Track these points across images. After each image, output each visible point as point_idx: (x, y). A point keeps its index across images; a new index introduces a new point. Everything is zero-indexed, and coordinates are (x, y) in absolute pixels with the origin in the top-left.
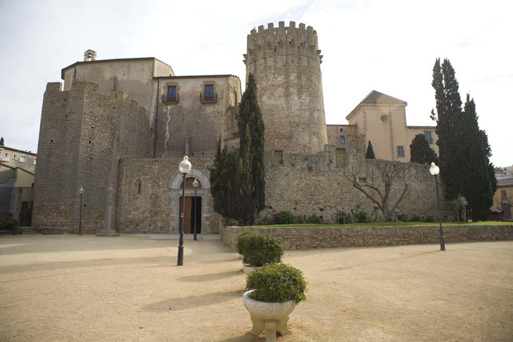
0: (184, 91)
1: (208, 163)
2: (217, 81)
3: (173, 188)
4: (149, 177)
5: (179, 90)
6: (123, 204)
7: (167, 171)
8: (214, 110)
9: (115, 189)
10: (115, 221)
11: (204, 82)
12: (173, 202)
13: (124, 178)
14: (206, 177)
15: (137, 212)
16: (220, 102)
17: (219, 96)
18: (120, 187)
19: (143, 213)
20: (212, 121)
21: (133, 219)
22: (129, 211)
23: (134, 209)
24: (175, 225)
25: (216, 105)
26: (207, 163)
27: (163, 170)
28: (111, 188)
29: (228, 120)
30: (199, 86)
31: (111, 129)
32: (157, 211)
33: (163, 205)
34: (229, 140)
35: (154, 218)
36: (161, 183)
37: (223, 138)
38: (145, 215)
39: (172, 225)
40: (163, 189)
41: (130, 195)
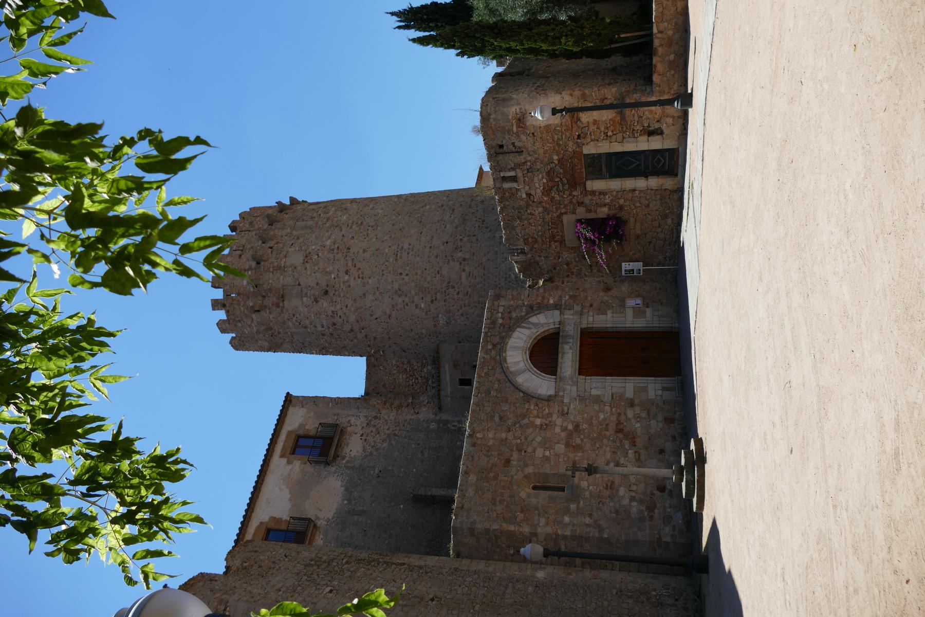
0: (288, 506)
1: (500, 315)
2: (292, 424)
3: (552, 392)
4: (515, 455)
5: (279, 521)
6: (594, 533)
7: (505, 407)
8: (359, 435)
11: (282, 456)
12: (594, 392)
13: (512, 528)
14: (533, 320)
15: (622, 491)
16: (343, 421)
17: (330, 421)
20: (384, 441)
21: (641, 502)
22: (617, 512)
23: (611, 497)
24: (659, 386)
25: (349, 429)
26: (496, 319)
27: (501, 418)
29: (392, 404)
30: (290, 467)
31: (347, 563)
32: (619, 431)
33: (602, 416)
34: (442, 393)
35: (639, 441)
36: (538, 421)
37: (433, 417)
39: (660, 393)
40: (555, 416)
41: (567, 511)
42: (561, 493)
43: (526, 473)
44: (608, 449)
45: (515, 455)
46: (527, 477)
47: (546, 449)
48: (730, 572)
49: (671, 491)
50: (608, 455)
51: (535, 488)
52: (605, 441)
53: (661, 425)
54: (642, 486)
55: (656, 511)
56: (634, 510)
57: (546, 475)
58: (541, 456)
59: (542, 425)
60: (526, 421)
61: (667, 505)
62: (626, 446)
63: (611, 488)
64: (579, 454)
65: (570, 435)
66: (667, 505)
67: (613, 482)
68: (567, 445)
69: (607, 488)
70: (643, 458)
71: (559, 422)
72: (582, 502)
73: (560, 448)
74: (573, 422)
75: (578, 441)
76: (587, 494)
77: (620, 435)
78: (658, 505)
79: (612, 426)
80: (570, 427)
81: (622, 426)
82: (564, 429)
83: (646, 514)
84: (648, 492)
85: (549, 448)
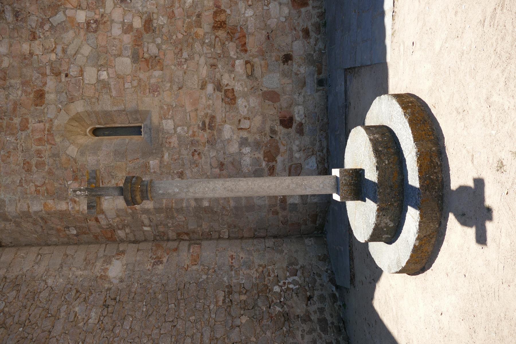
4: (51, 83)
9: (123, 252)
10: (270, 243)
13: (63, 206)
15: (227, 131)
18: (112, 229)
19: (230, 97)
21: (257, 145)
23: (211, 142)
28: (116, 270)
32: (219, 25)
36: (81, 16)
38: (238, 87)
42: (136, 138)
43: (73, 113)
44: (202, 60)
45: (51, 83)
46: (77, 118)
47: (100, 67)
48: (365, 201)
49: (301, 125)
50: (204, 71)
51: (96, 132)
52: (197, 46)
53: (286, 10)
54: (258, 120)
55: (279, 159)
56: (247, 160)
57: (107, 114)
58: (94, 81)
59: (88, 24)
60: (60, 17)
61: (295, 148)
62: (232, 54)
63: (211, 128)
64: (157, 73)
65: (138, 41)
66: (295, 148)
67: (213, 118)
68: (136, 58)
69: (203, 129)
70: (258, 72)
71: (117, 14)
72: (166, 156)
73: (124, 64)
74: (141, 14)
75: (154, 50)
76: (174, 140)
77: (222, 34)
78: (282, 149)
79: (208, 18)
80: (138, 23)
81: (222, 17)
82: (128, 28)
83: (264, 164)
84: (268, 129)
85: (106, 66)
